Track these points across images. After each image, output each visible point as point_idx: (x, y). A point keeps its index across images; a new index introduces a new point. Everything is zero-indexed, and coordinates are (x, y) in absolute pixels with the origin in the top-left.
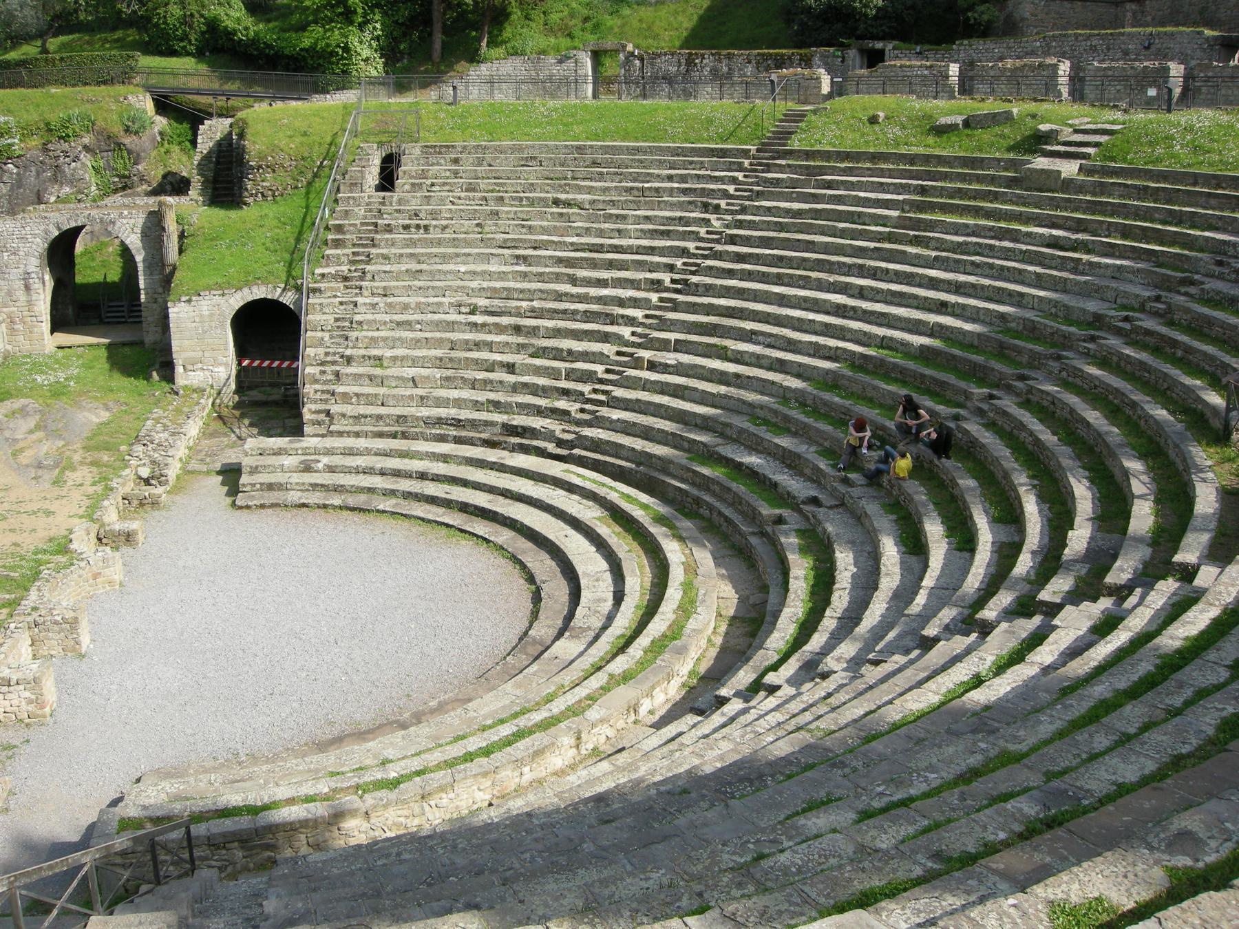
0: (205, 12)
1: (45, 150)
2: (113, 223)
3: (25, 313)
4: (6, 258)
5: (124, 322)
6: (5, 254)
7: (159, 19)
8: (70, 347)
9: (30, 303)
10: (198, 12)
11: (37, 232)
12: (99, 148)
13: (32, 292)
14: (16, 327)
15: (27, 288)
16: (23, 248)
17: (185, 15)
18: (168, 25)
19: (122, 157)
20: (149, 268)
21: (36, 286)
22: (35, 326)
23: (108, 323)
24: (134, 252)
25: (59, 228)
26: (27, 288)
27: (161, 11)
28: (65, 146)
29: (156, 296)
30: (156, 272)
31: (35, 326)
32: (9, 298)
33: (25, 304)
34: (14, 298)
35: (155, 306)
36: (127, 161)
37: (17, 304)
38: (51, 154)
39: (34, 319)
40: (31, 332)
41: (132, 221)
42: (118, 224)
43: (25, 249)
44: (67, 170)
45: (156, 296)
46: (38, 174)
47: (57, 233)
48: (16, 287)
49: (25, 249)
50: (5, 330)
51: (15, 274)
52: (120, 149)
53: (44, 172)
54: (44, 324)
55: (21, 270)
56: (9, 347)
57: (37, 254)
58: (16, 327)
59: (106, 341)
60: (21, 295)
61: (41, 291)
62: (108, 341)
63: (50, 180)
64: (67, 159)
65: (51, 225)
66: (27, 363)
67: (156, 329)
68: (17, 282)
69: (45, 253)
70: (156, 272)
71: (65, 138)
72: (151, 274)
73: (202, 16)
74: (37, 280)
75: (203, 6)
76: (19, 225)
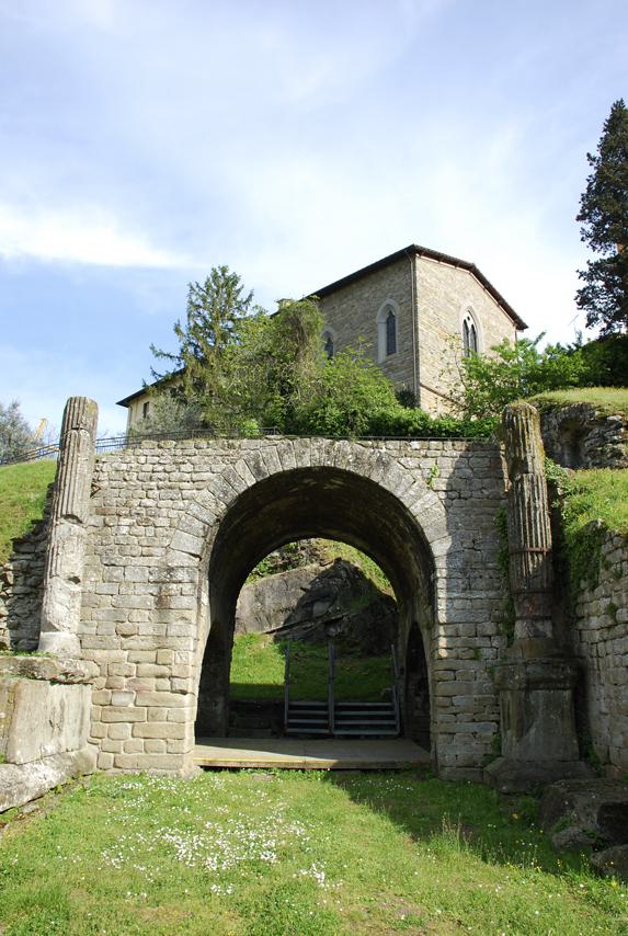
0: (368, 411)
2: (383, 464)
3: (145, 667)
4: (125, 530)
5: (331, 736)
6: (127, 521)
7: (315, 421)
8: (234, 770)
9: (161, 643)
10: (362, 412)
11: (206, 476)
13: (173, 615)
14: (118, 699)
15: (162, 603)
16: (167, 512)
17: (346, 414)
18: (326, 425)
20: (463, 571)
21: (186, 601)
22: (166, 704)
23: (294, 736)
24: (429, 533)
25: (258, 471)
26: (162, 603)
27: (319, 411)
29: (478, 642)
30: (481, 583)
31: (166, 704)
32: (113, 626)
33: (150, 643)
34: (126, 628)
35: (473, 666)
37: (129, 643)
39: (166, 683)
40: (152, 717)
41: (430, 463)
42: (396, 468)
43: (173, 514)
45: (478, 642)
47: (251, 481)
48: (136, 600)
49: (173, 514)
50: (89, 705)
51: (137, 571)
54: (187, 698)
55: (153, 562)
56: (91, 751)
57: (198, 525)
58: (118, 699)
59: (327, 762)
60: (144, 622)
61: (192, 615)
62: (327, 762)
65: (240, 465)
66: (134, 795)
67: (474, 727)
68: (141, 589)
69: (216, 530)
70: (481, 583)
72: (468, 588)
73: (365, 415)
74: (187, 588)
76: (168, 459)
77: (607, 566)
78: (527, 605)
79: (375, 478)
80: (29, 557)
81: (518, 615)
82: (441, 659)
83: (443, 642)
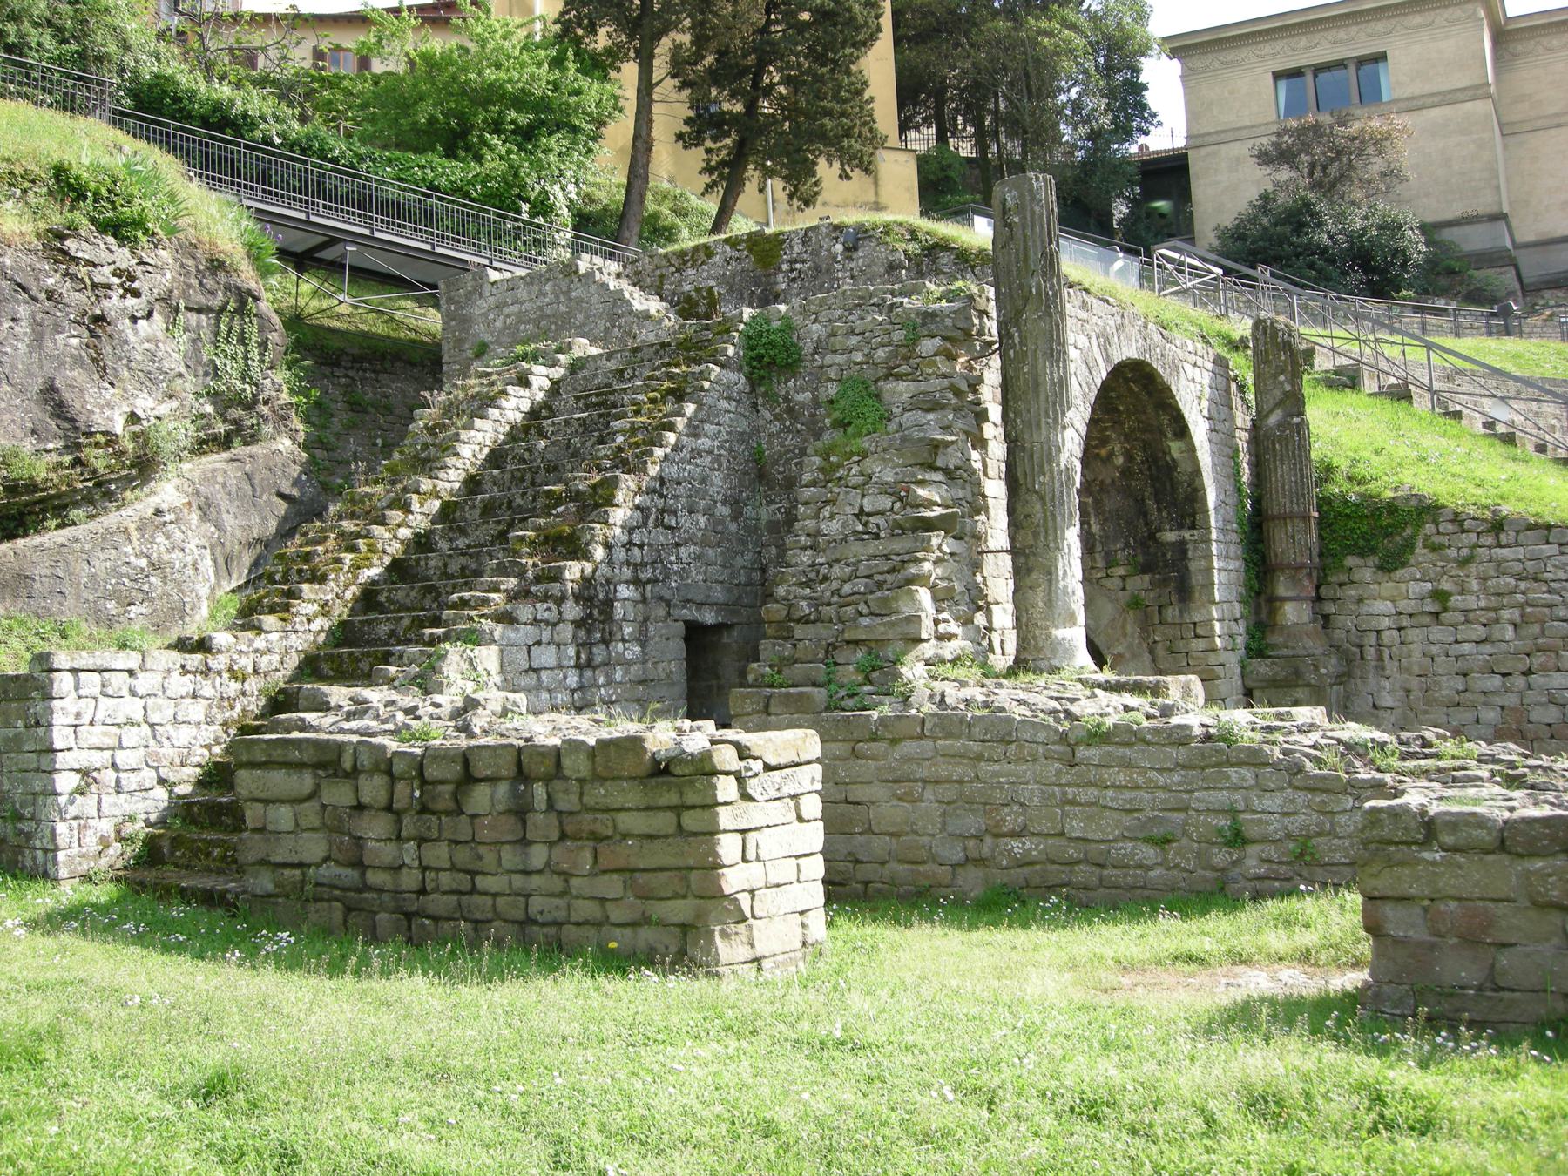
1: (55, 244)
12: (184, 295)
17: (82, 55)
19: (242, 340)
25: (1108, 359)
28: (123, 257)
36: (255, 353)
38: (82, 271)
44: (131, 338)
46: (38, 340)
52: (241, 310)
53: (58, 329)
63: (78, 361)
64: (131, 301)
71: (118, 229)
75: (126, 47)
77: (1435, 548)
78: (1306, 582)
79: (1174, 389)
80: (938, 476)
81: (1281, 591)
82: (1214, 650)
83: (1217, 626)
